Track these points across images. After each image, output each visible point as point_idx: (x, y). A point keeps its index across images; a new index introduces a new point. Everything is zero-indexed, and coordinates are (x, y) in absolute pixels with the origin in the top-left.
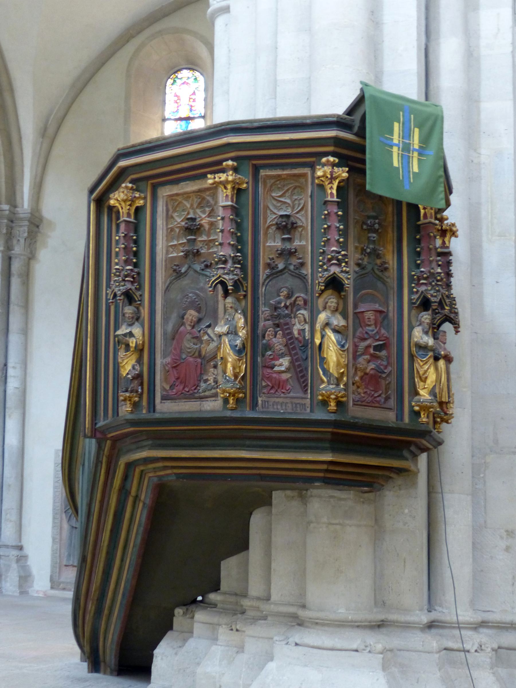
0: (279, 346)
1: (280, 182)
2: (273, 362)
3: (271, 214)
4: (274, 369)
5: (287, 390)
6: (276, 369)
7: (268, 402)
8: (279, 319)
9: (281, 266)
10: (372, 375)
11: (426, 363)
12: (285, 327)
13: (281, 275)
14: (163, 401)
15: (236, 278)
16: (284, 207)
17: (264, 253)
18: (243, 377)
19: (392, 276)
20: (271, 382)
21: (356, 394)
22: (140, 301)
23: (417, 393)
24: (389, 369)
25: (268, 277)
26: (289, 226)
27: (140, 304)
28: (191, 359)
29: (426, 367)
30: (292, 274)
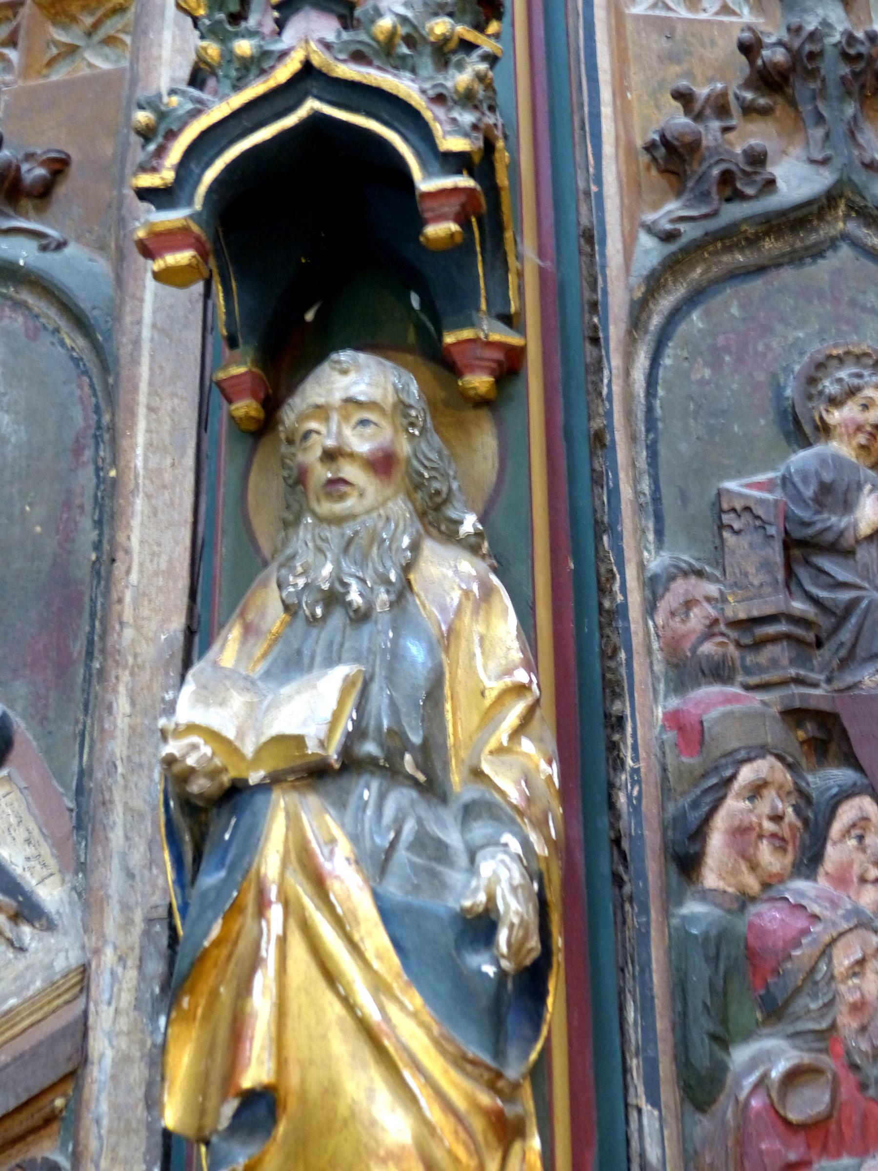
8: (844, 664)
13: (796, 259)
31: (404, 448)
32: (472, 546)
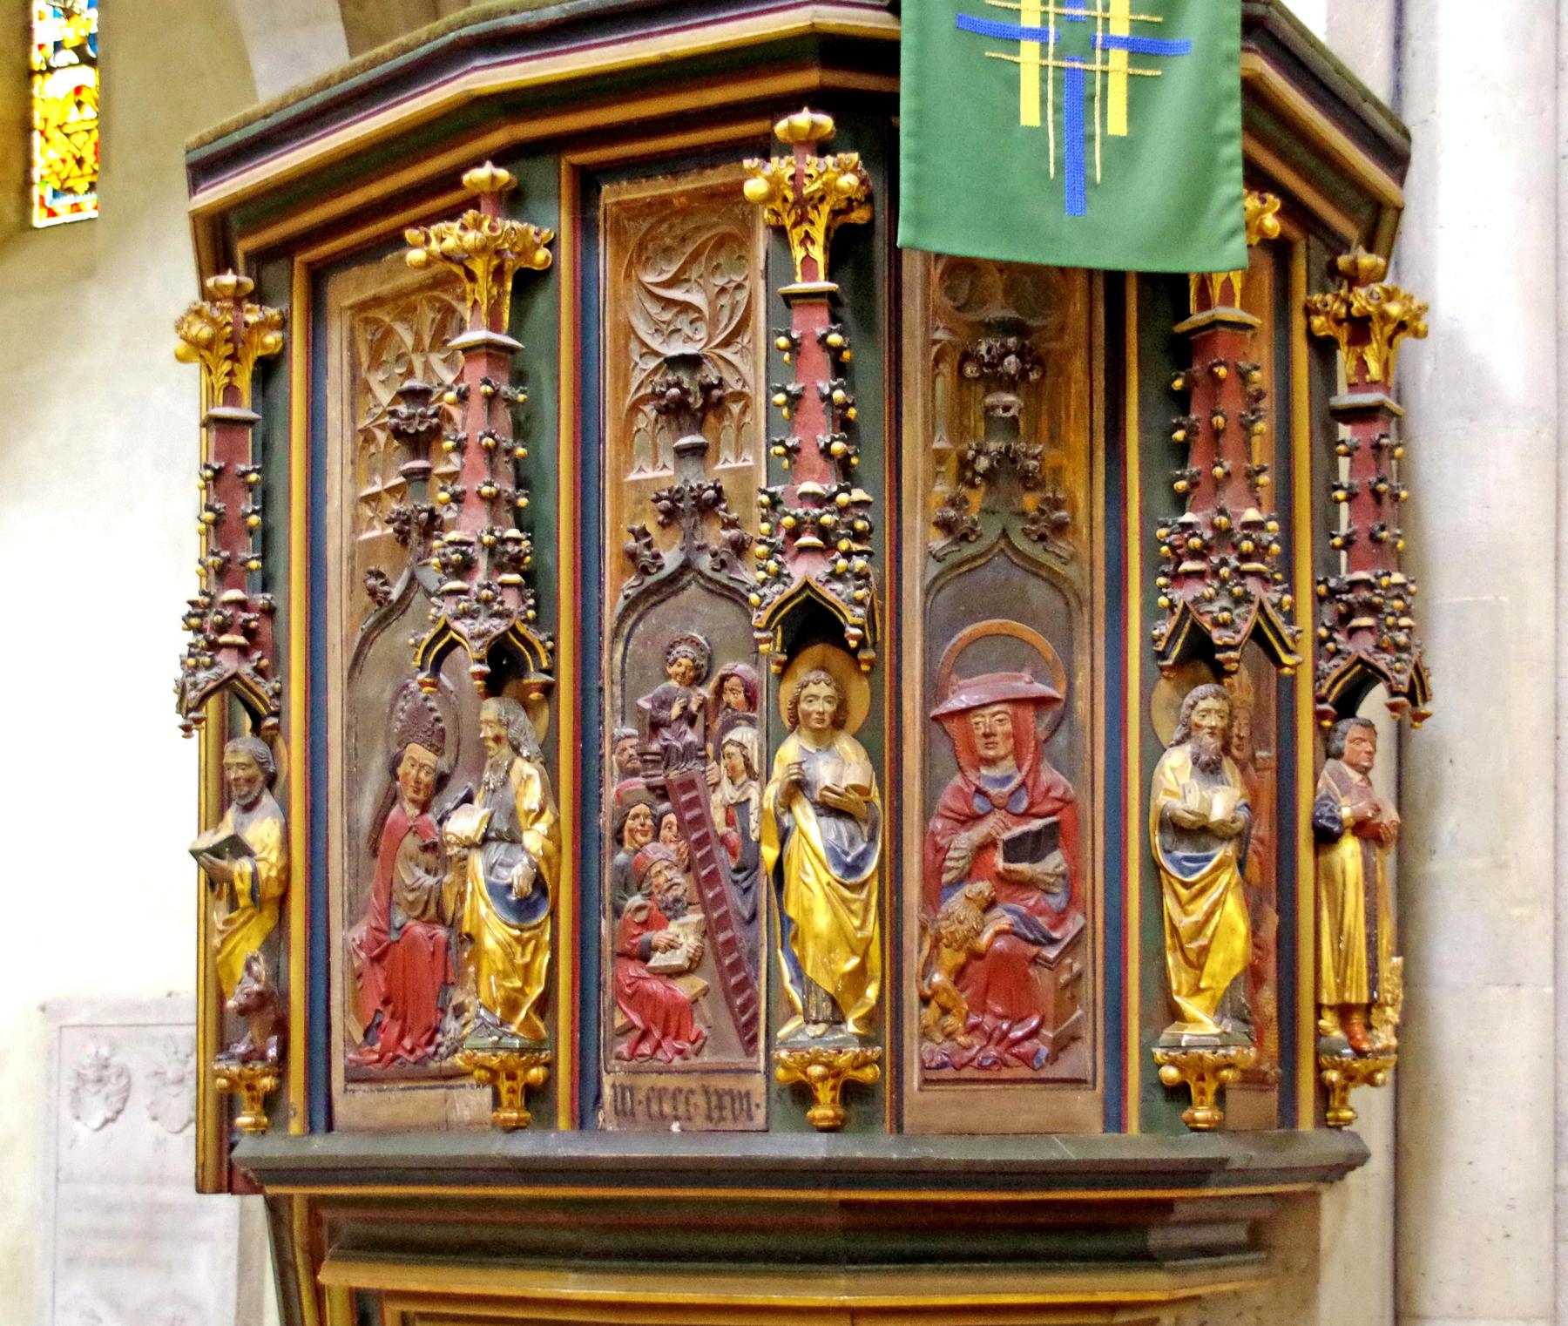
0: (666, 872)
1: (671, 227)
2: (647, 935)
3: (642, 356)
4: (652, 963)
5: (693, 1043)
6: (658, 960)
7: (632, 1090)
9: (671, 559)
10: (1001, 955)
11: (1203, 891)
12: (684, 798)
14: (350, 1086)
15: (498, 626)
16: (682, 322)
17: (618, 509)
18: (545, 1005)
19: (1084, 553)
20: (640, 1011)
21: (939, 1037)
22: (276, 714)
23: (1175, 1014)
24: (1075, 923)
25: (632, 604)
26: (696, 401)
27: (276, 727)
28: (419, 930)
29: (1204, 904)
30: (709, 586)
31: (503, 732)
32: (528, 759)
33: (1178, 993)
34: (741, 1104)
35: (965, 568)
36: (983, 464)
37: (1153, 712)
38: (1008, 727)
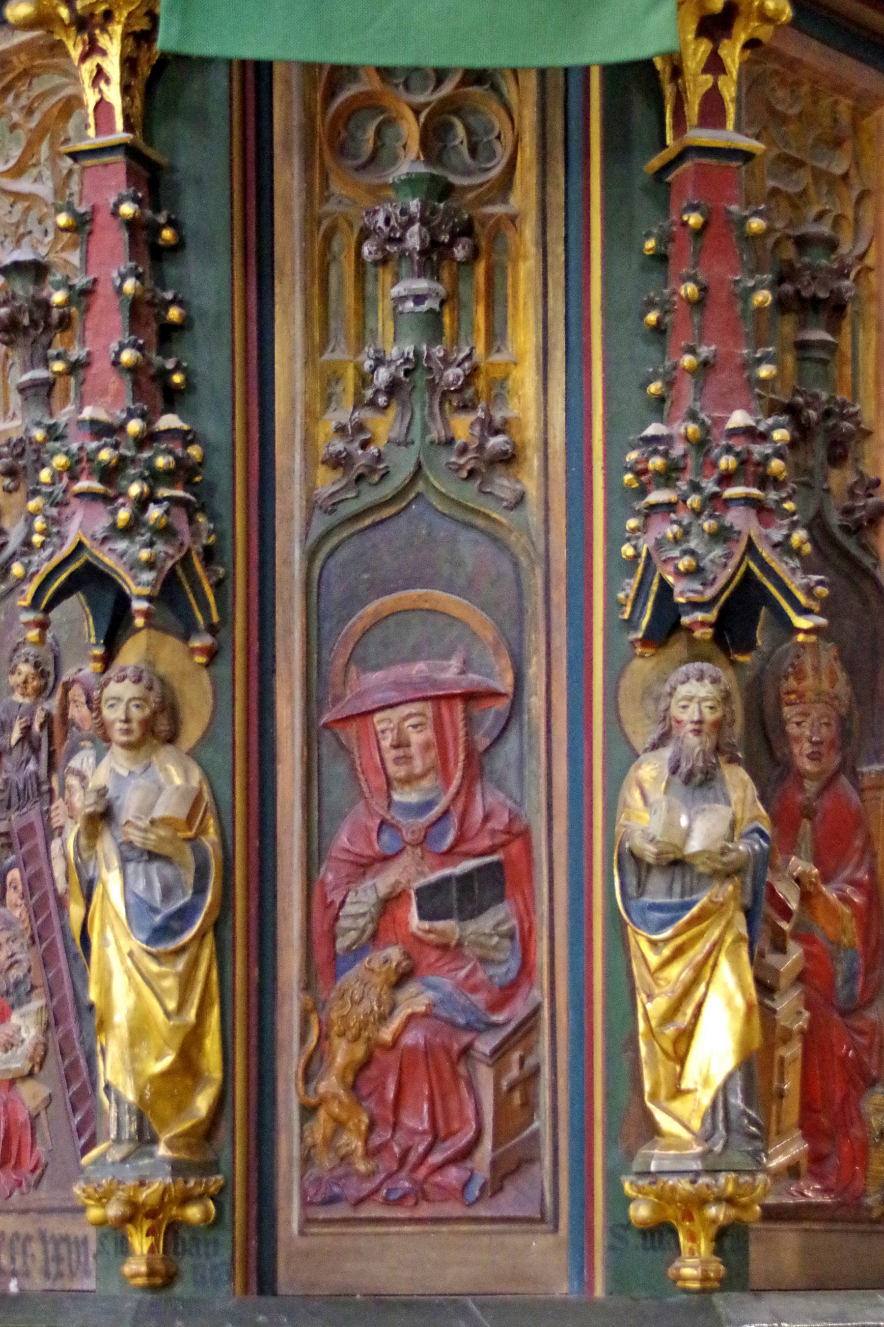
11: (678, 953)
33: (654, 1096)
34: (79, 1257)
35: (368, 521)
36: (383, 375)
37: (622, 706)
38: (429, 734)
